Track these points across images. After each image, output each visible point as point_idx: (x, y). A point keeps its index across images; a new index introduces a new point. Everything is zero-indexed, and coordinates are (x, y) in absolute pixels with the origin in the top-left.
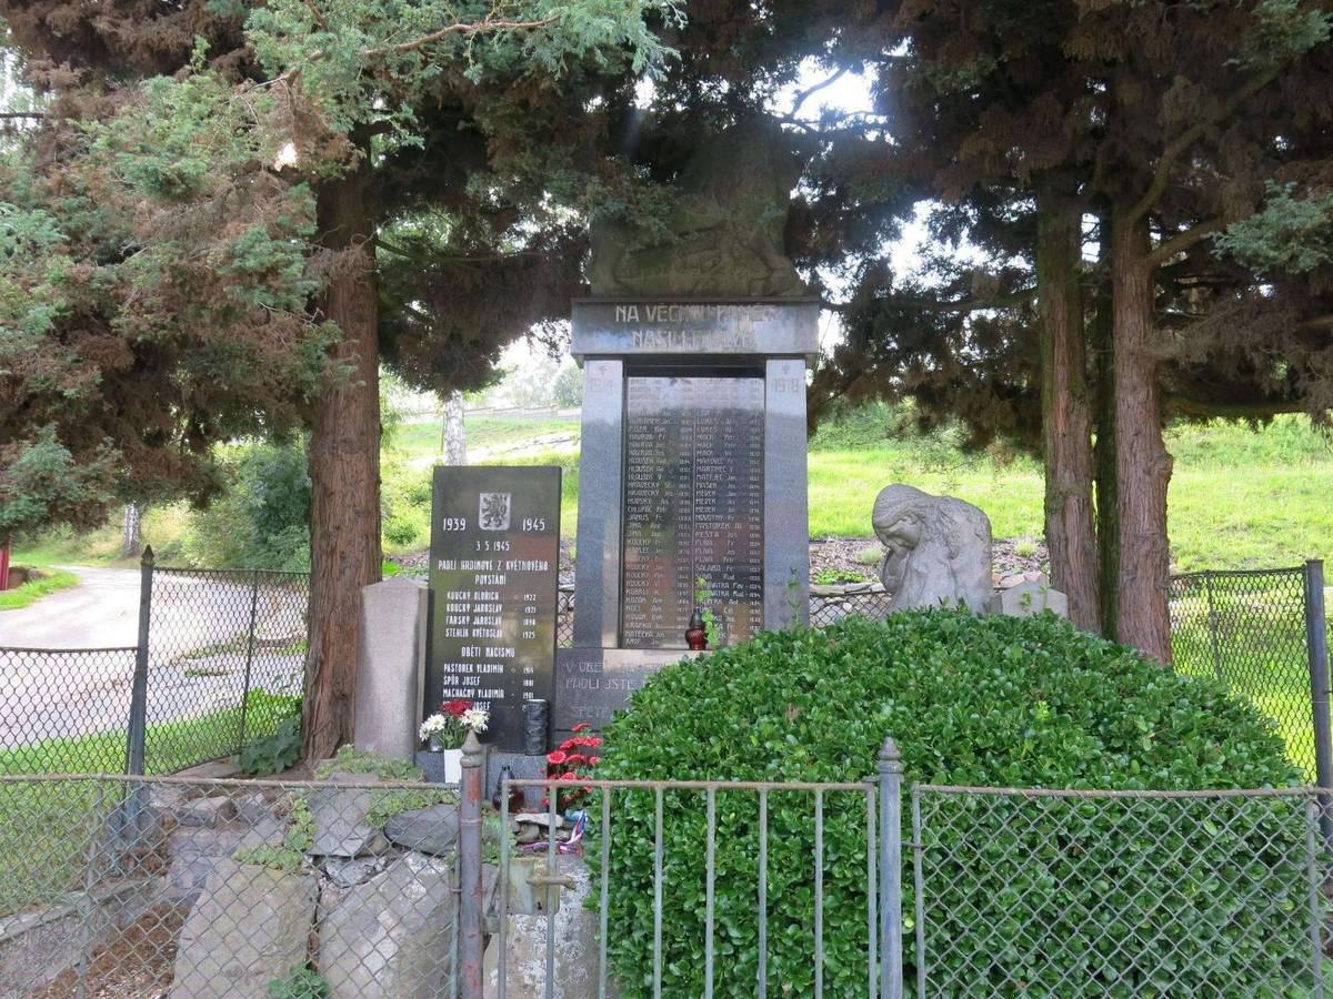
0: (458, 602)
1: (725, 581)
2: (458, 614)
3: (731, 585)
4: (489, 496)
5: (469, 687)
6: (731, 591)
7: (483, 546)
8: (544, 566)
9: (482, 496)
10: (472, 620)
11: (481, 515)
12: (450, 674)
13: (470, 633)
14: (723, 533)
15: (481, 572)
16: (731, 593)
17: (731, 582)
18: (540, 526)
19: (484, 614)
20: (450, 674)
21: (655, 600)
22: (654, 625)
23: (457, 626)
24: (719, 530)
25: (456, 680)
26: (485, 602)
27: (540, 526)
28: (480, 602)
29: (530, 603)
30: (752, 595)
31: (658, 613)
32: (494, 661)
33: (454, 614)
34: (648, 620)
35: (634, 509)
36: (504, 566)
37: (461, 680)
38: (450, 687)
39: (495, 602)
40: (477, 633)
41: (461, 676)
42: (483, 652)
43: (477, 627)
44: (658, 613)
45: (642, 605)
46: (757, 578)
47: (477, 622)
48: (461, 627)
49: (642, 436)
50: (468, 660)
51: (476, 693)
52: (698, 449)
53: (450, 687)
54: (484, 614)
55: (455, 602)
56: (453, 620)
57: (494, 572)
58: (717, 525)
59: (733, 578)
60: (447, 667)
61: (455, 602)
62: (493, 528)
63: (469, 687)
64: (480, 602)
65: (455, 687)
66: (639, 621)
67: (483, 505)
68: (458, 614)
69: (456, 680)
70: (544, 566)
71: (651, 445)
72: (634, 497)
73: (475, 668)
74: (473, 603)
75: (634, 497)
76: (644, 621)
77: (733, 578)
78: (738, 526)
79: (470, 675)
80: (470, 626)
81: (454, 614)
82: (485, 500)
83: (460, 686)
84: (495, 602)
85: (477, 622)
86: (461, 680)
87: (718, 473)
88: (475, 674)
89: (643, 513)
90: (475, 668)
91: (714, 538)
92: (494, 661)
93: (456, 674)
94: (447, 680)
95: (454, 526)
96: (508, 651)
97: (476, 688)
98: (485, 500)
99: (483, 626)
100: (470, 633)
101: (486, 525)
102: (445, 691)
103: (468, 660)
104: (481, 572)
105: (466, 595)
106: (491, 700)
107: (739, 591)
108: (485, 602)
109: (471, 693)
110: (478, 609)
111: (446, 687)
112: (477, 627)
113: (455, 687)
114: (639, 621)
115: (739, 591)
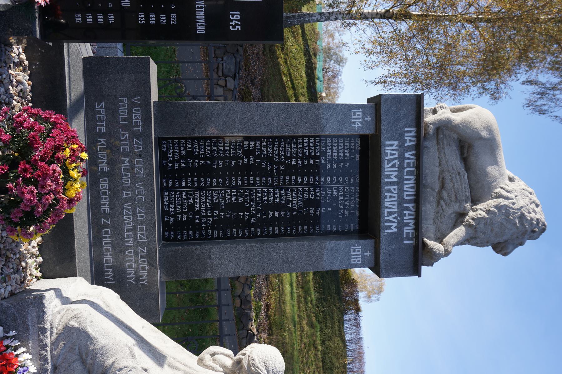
1: (213, 213)
3: (210, 217)
6: (206, 217)
8: (201, 30)
14: (248, 209)
16: (204, 217)
17: (212, 216)
18: (234, 27)
21: (196, 161)
22: (178, 161)
24: (250, 206)
27: (234, 27)
29: (168, 19)
30: (203, 232)
31: (186, 164)
34: (182, 157)
35: (264, 143)
44: (186, 164)
45: (192, 152)
46: (216, 235)
49: (318, 148)
52: (309, 190)
58: (254, 205)
59: (215, 218)
66: (180, 150)
70: (201, 30)
71: (312, 154)
72: (273, 143)
75: (273, 143)
76: (180, 153)
77: (215, 218)
78: (253, 220)
87: (292, 204)
89: (261, 151)
91: (243, 203)
107: (206, 223)
114: (180, 150)
115: (206, 223)
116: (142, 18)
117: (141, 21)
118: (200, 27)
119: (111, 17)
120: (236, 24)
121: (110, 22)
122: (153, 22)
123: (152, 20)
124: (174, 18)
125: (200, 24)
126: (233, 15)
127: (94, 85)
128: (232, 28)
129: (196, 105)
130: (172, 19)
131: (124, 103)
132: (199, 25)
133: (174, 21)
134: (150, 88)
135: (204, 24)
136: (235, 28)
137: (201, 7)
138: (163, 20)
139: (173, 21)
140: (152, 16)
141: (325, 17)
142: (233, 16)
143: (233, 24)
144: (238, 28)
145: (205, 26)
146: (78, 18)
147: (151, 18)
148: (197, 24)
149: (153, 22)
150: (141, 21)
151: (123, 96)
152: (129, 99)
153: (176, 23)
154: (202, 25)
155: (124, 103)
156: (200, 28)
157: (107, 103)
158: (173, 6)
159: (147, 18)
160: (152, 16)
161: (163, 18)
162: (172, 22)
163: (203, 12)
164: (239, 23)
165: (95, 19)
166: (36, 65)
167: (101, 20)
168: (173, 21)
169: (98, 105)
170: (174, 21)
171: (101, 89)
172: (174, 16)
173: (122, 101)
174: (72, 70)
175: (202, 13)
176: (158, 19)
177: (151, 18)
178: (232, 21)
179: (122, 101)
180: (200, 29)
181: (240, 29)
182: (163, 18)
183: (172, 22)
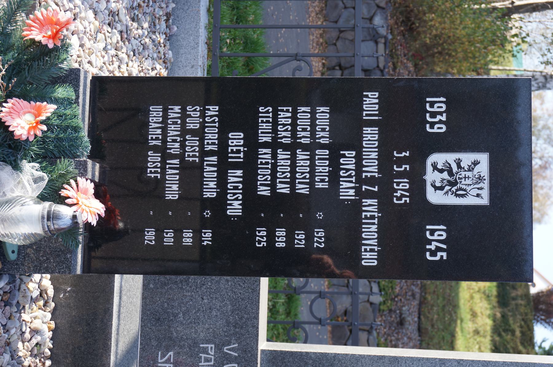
0: (313, 125)
2: (294, 124)
4: (483, 168)
5: (183, 146)
7: (400, 162)
9: (484, 158)
10: (285, 147)
11: (451, 158)
12: (203, 115)
13: (265, 145)
15: (359, 159)
19: (293, 166)
20: (203, 115)
23: (275, 123)
25: (193, 124)
26: (312, 166)
28: (312, 159)
32: (222, 181)
33: (294, 118)
36: (370, 195)
37: (193, 132)
38: (184, 116)
39: (312, 184)
40: (265, 154)
41: (200, 133)
42: (236, 166)
43: (274, 156)
47: (282, 155)
48: (275, 131)
50: (223, 142)
51: (174, 157)
53: (184, 116)
54: (293, 166)
55: (313, 119)
56: (285, 116)
57: (360, 181)
60: (213, 110)
61: (313, 119)
62: (431, 176)
63: (183, 146)
64: (312, 159)
65: (184, 123)
67: (467, 158)
68: (294, 124)
69: (193, 124)
73: (211, 153)
74: (311, 148)
79: (202, 146)
80: (275, 145)
81: (294, 118)
82: (476, 163)
83: (184, 132)
84: (312, 184)
85: (282, 155)
86: (193, 132)
88: (204, 153)
90: (211, 153)
92: (222, 181)
93: (203, 125)
94: (194, 112)
95: (434, 115)
96: (236, 204)
97: (181, 156)
98: (476, 163)
99: (275, 166)
100: (265, 145)
101: (435, 167)
102: (177, 109)
103: (223, 142)
104: (359, 159)
105: (324, 137)
106: (163, 179)
108: (312, 166)
109: (175, 148)
110: (301, 155)
111: (184, 110)
112: (274, 156)
113: (184, 123)
116: (262, 237)
117: (260, 242)
118: (368, 254)
119: (207, 235)
120: (438, 249)
121: (205, 243)
122: (281, 244)
123: (280, 240)
124: (320, 238)
125: (368, 248)
126: (432, 232)
127: (159, 319)
128: (431, 255)
129: (339, 361)
130: (316, 239)
131: (209, 354)
132: (366, 250)
133: (320, 243)
134: (258, 328)
135: (376, 248)
136: (436, 256)
137: (373, 217)
138: (300, 240)
139: (317, 242)
140: (281, 233)
141: (538, 84)
142: (432, 233)
143: (433, 247)
144: (442, 256)
145: (378, 251)
146: (150, 236)
147: (279, 237)
148: (363, 247)
149: (281, 244)
150: (260, 242)
151: (208, 342)
152: (219, 348)
153: (323, 246)
154: (372, 250)
155: (209, 354)
156: (368, 255)
157: (179, 353)
158: (320, 216)
159: (271, 237)
160: (281, 233)
161: (300, 236)
162: (316, 244)
163: (376, 226)
164: (444, 247)
165: (178, 237)
166: (65, 292)
167: (188, 240)
168: (317, 242)
169: (163, 356)
170: (320, 243)
171: (170, 327)
172: (320, 233)
173: (205, 351)
174: (124, 298)
175: (374, 228)
176: (290, 238)
177: (279, 237)
178: (430, 242)
179: (205, 351)
180: (368, 257)
181: (445, 258)
182: (300, 236)
183: (316, 244)
